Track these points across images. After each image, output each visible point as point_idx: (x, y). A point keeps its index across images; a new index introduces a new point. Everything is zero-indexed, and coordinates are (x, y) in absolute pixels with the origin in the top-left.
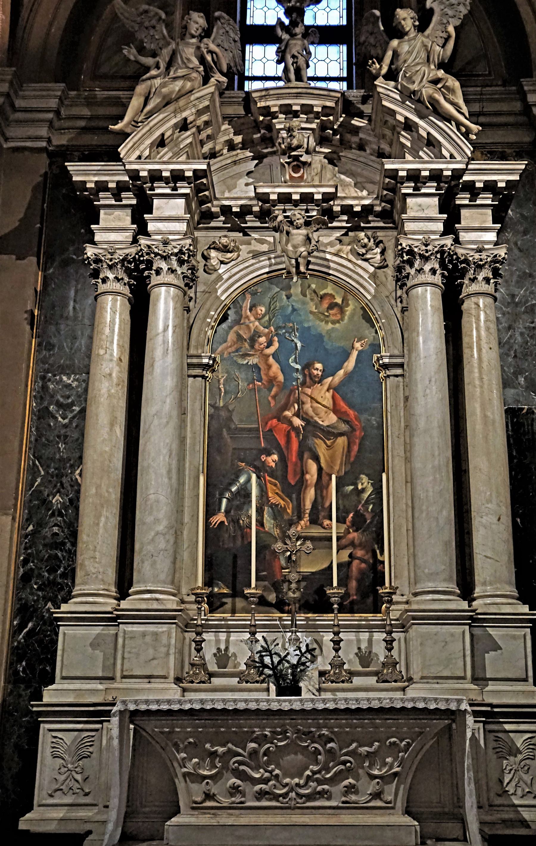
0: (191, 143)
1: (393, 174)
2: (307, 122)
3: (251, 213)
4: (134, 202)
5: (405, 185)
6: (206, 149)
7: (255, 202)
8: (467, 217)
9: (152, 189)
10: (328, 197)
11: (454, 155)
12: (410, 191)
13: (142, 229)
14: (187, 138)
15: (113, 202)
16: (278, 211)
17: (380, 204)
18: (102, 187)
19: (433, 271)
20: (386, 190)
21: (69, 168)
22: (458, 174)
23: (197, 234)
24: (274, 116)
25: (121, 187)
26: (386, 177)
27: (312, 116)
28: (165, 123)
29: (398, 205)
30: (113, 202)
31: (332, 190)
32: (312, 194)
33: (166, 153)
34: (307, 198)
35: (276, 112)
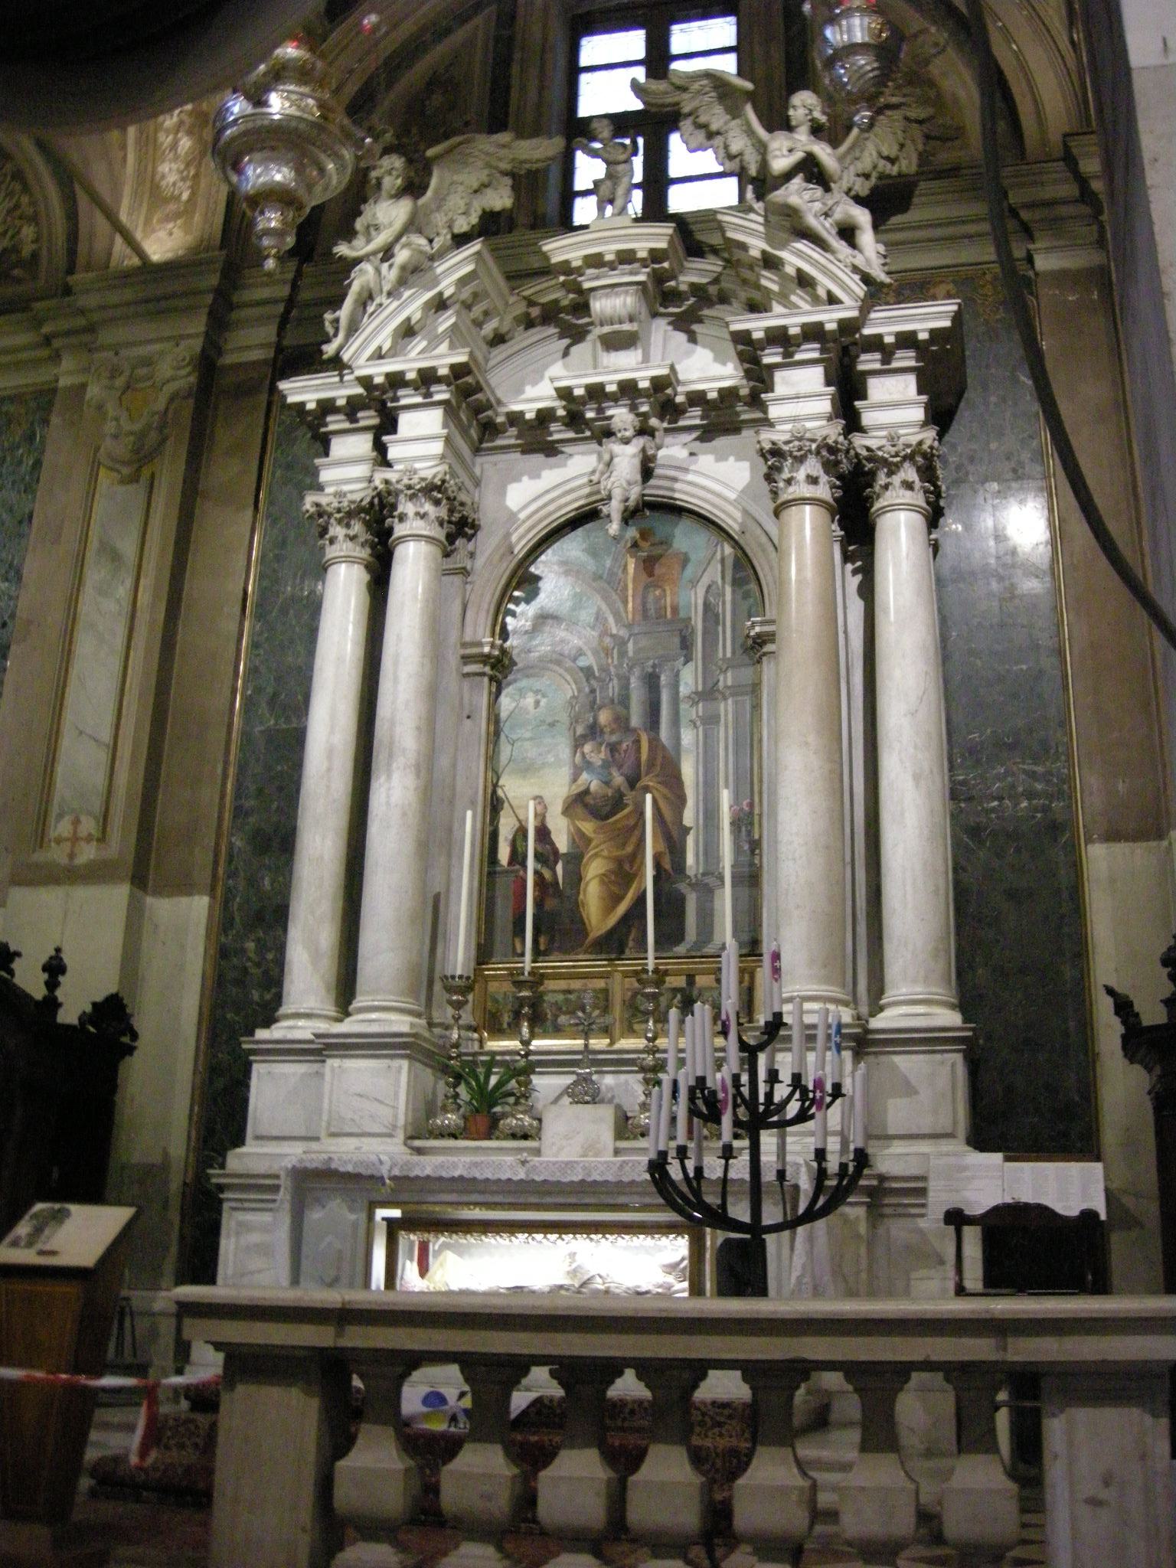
0: (454, 325)
4: (375, 421)
8: (880, 389)
9: (396, 399)
13: (381, 458)
14: (446, 321)
15: (347, 425)
24: (579, 271)
27: (636, 265)
28: (413, 305)
30: (347, 425)
33: (419, 344)
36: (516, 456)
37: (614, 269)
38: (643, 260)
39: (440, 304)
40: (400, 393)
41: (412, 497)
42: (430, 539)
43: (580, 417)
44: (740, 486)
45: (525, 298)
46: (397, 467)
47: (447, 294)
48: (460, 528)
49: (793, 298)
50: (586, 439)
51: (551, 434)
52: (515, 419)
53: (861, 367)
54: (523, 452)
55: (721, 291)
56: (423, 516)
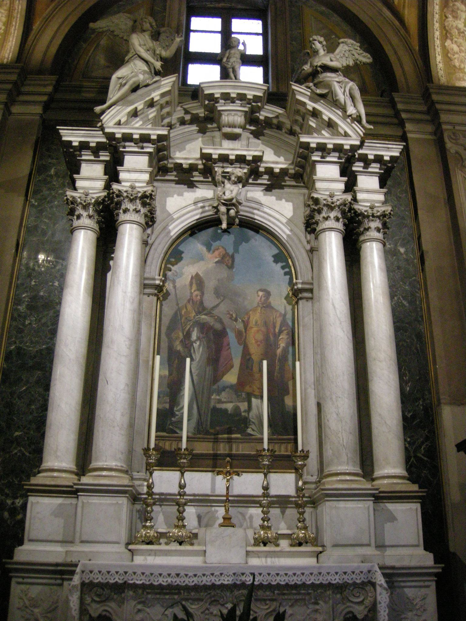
1: (306, 146)
2: (241, 106)
3: (197, 170)
4: (107, 158)
5: (314, 154)
6: (166, 121)
7: (200, 162)
10: (258, 159)
11: (351, 135)
12: (318, 159)
15: (92, 158)
16: (218, 170)
17: (294, 169)
18: (84, 146)
20: (300, 157)
21: (61, 131)
22: (354, 148)
23: (156, 184)
24: (216, 100)
25: (100, 147)
26: (301, 147)
29: (308, 170)
30: (92, 158)
32: (245, 156)
34: (241, 159)
35: (218, 98)
36: (173, 185)
37: (234, 102)
38: (250, 99)
39: (151, 104)
40: (127, 144)
41: (131, 201)
43: (206, 170)
45: (184, 109)
46: (123, 184)
47: (155, 99)
49: (323, 132)
50: (209, 182)
51: (193, 177)
53: (354, 169)
54: (176, 184)
55: (279, 122)
56: (137, 211)
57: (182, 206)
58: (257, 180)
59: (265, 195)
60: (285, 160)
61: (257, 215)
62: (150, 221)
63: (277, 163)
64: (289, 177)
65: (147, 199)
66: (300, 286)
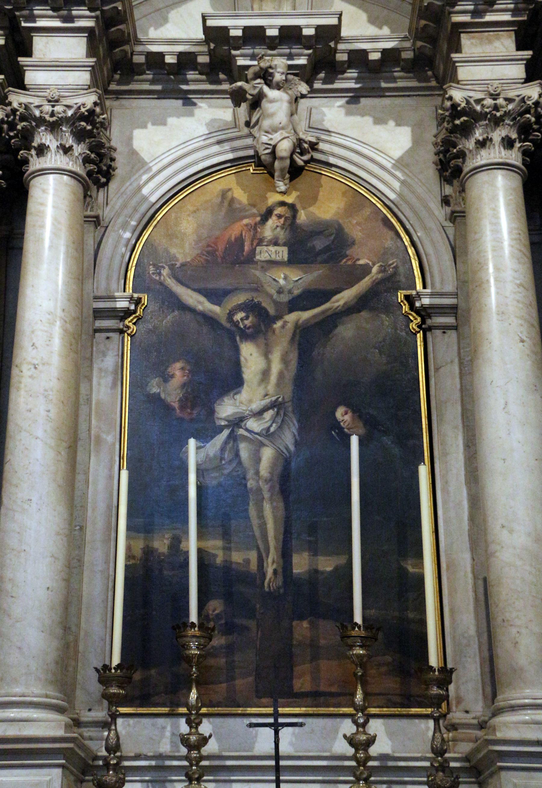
19: (508, 143)
31: (334, 21)
34: (290, 36)
42: (73, 175)
44: (397, 153)
48: (98, 172)
52: (155, 60)
57: (170, 141)
58: (332, 83)
59: (349, 113)
60: (392, 31)
61: (333, 155)
62: (98, 172)
63: (374, 39)
64: (403, 70)
65: (89, 128)
66: (426, 301)
